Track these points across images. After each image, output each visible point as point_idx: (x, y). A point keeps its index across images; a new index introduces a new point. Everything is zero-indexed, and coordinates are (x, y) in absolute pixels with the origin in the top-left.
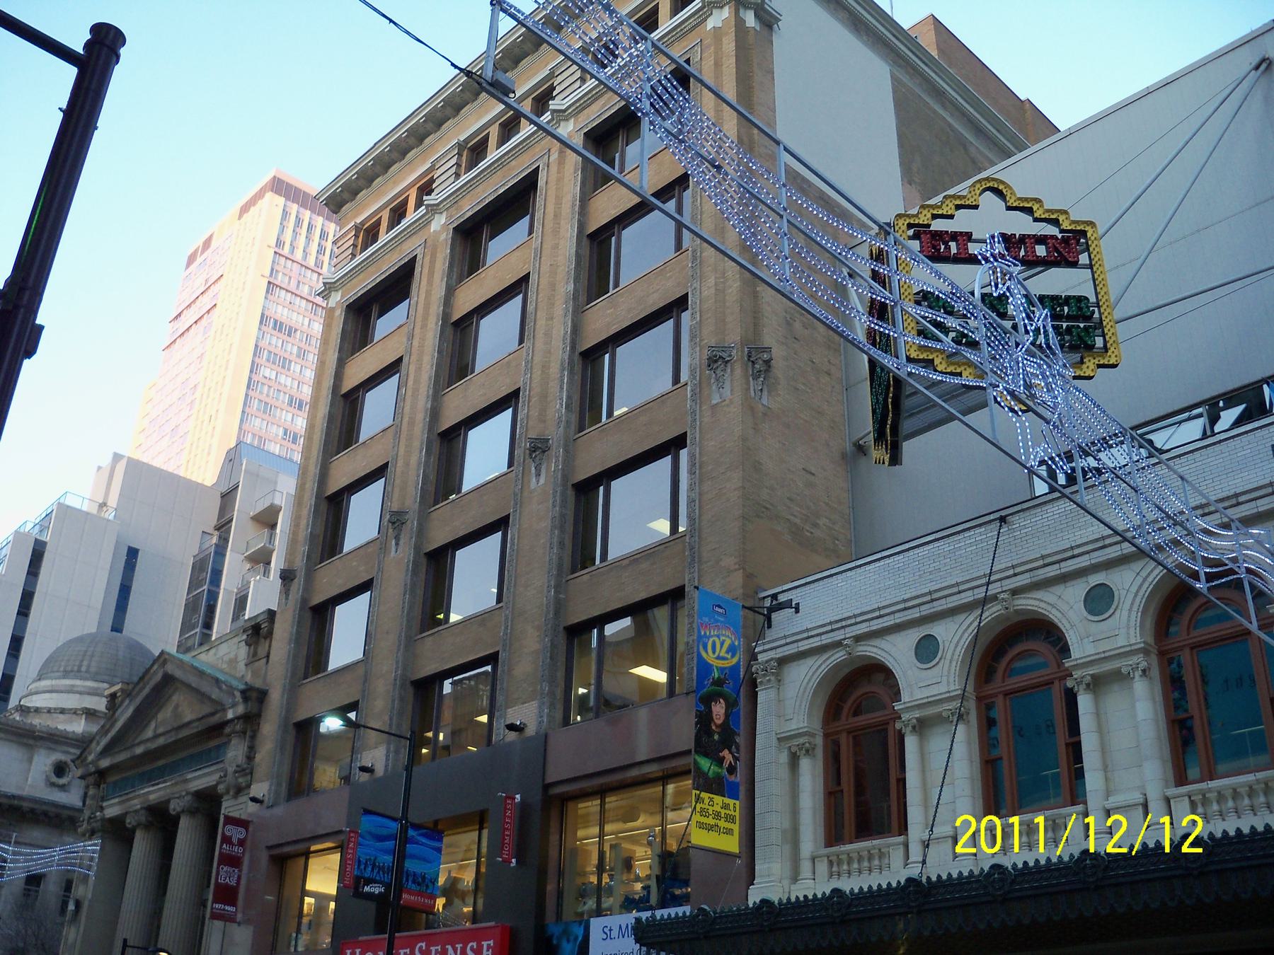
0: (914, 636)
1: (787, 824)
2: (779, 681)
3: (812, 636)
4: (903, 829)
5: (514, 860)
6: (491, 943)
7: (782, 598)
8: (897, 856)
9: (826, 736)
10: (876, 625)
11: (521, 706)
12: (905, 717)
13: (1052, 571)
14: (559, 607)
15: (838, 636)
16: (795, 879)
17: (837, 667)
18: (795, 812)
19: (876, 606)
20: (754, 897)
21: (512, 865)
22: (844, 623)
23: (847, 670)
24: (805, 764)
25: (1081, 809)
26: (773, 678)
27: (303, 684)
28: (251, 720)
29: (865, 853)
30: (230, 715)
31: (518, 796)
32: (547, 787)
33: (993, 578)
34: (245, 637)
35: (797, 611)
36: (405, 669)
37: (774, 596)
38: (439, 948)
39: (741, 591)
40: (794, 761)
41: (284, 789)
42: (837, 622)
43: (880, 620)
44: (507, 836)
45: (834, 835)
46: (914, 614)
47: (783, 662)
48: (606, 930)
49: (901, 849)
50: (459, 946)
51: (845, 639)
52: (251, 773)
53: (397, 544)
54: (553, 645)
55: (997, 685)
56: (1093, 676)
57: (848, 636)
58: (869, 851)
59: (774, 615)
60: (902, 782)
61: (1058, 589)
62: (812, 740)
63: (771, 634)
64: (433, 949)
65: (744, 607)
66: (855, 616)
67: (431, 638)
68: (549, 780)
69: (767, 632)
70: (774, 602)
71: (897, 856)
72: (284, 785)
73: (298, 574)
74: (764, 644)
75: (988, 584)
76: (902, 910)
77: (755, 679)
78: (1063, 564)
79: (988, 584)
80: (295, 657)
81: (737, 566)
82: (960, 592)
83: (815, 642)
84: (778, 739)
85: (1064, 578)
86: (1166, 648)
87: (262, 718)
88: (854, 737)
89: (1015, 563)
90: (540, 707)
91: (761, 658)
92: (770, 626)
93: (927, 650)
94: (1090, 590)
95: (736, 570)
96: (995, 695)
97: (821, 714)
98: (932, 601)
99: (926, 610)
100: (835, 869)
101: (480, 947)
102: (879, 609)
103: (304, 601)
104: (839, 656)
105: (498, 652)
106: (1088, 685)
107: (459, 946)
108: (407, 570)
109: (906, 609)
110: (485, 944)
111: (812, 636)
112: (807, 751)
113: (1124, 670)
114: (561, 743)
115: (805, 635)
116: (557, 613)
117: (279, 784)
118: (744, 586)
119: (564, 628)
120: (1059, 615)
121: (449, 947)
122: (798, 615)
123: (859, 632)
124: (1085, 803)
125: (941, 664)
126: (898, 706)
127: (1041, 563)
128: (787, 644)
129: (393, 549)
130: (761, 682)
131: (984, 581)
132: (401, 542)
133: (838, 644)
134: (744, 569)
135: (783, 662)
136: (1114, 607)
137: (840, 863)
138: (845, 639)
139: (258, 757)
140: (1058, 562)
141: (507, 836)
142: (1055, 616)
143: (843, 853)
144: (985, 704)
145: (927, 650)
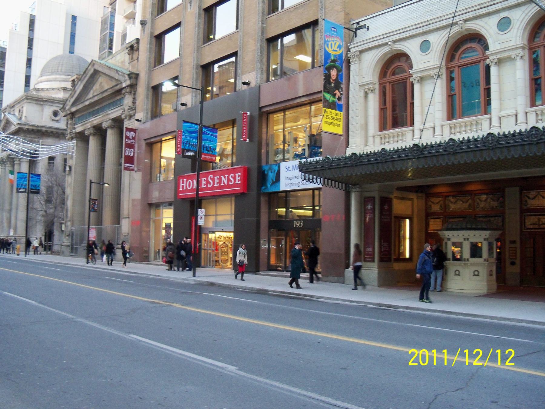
0: (420, 40)
1: (363, 122)
3: (375, 41)
4: (412, 124)
5: (248, 140)
6: (240, 174)
7: (361, 24)
8: (409, 135)
9: (380, 84)
10: (403, 36)
11: (249, 74)
12: (414, 76)
13: (484, 11)
15: (386, 41)
16: (366, 145)
17: (386, 54)
18: (366, 117)
19: (403, 27)
20: (349, 152)
21: (247, 142)
22: (389, 35)
23: (389, 56)
24: (371, 96)
25: (489, 116)
26: (357, 59)
27: (154, 70)
28: (133, 87)
29: (396, 134)
30: (124, 85)
31: (248, 113)
32: (261, 108)
33: (456, 14)
34: (127, 51)
35: (368, 29)
36: (197, 61)
37: (358, 23)
38: (218, 177)
39: (343, 21)
40: (366, 94)
41: (149, 115)
42: (386, 34)
43: (405, 33)
45: (383, 127)
46: (420, 30)
47: (361, 52)
48: (287, 167)
49: (411, 132)
50: (226, 176)
51: (389, 42)
52: (135, 109)
53: (191, 6)
54: (262, 48)
55: (455, 62)
56: (498, 59)
57: (390, 40)
58: (397, 133)
59: (358, 32)
60: (412, 104)
61: (486, 19)
62: (374, 86)
63: (356, 40)
65: (344, 28)
66: (394, 31)
67: (208, 46)
68: (261, 105)
69: (355, 38)
70: (358, 26)
71: (409, 135)
72: (149, 113)
73: (148, 21)
75: (454, 17)
76: (411, 157)
77: (349, 60)
78: (489, 8)
79: (454, 17)
80: (150, 58)
81: (341, 10)
82: (441, 21)
83: (376, 43)
84: (360, 85)
85: (489, 14)
86: (532, 47)
87: (138, 86)
88: (392, 85)
89: (467, 7)
90: (256, 74)
91: (351, 50)
92: (356, 37)
93: (425, 46)
94: (501, 19)
95: (342, 11)
96: (454, 67)
97: (378, 76)
98: (429, 24)
99: (426, 29)
100: (383, 141)
101: (235, 176)
102: (405, 28)
103: (152, 33)
104: (386, 49)
106: (496, 63)
107: (226, 176)
108: (196, 17)
109: (416, 28)
110: (237, 174)
111: (375, 41)
112: (372, 91)
113: (513, 56)
114: (266, 88)
115: (371, 40)
116: (263, 33)
117: (147, 113)
118: (345, 19)
120: (485, 31)
121: (222, 176)
123: (395, 39)
124: (490, 114)
125: (431, 53)
127: (478, 7)
128: (363, 44)
130: (352, 61)
131: (452, 15)
132: (192, 4)
133: (386, 44)
134: (345, 11)
135: (361, 52)
136: (511, 27)
137: (385, 138)
138: (389, 42)
139: (138, 102)
141: (245, 129)
142: (483, 32)
143: (386, 134)
144: (450, 71)
145: (425, 46)
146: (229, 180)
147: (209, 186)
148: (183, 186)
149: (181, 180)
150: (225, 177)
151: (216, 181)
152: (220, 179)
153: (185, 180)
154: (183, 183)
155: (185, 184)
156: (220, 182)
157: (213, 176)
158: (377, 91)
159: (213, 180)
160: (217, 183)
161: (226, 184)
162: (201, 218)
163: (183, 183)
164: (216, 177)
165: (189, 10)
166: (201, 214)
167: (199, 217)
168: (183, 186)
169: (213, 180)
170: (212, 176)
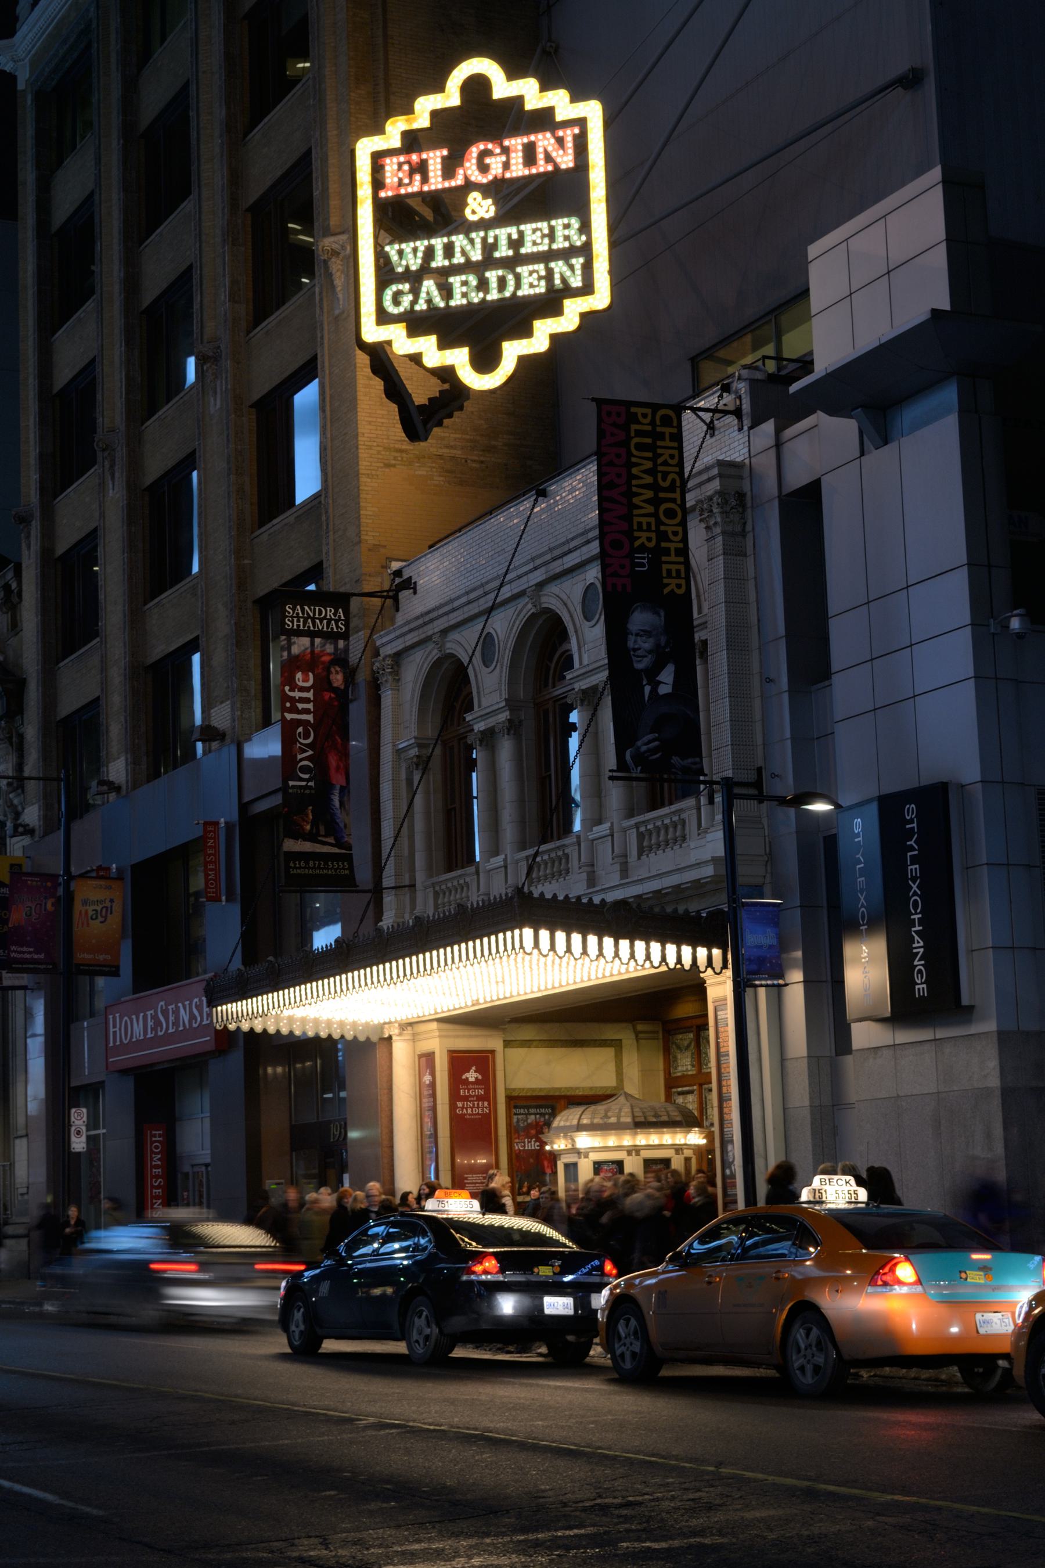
2: (399, 680)
14: (242, 579)
17: (437, 664)
35: (415, 593)
38: (173, 1006)
44: (211, 870)
50: (187, 1003)
63: (400, 618)
64: (170, 1007)
68: (247, 798)
74: (395, 630)
89: (552, 545)
90: (233, 710)
92: (397, 610)
105: (198, 636)
107: (187, 1003)
119: (255, 602)
121: (180, 1005)
122: (417, 596)
126: (469, 717)
129: (111, 486)
132: (117, 475)
135: (398, 657)
140: (446, 614)
141: (211, 870)
146: (192, 1017)
147: (160, 1034)
148: (115, 1033)
149: (111, 1017)
150: (185, 1008)
151: (171, 1018)
152: (176, 1012)
153: (117, 1015)
154: (114, 1026)
155: (117, 1029)
156: (176, 1023)
157: (167, 1005)
158: (436, 764)
159: (165, 1013)
160: (173, 1024)
161: (188, 1027)
162: (78, 1133)
163: (114, 1026)
164: (170, 1007)
165: (111, 491)
166: (77, 1122)
167: (73, 1129)
168: (115, 1033)
169: (165, 1013)
170: (162, 1003)
